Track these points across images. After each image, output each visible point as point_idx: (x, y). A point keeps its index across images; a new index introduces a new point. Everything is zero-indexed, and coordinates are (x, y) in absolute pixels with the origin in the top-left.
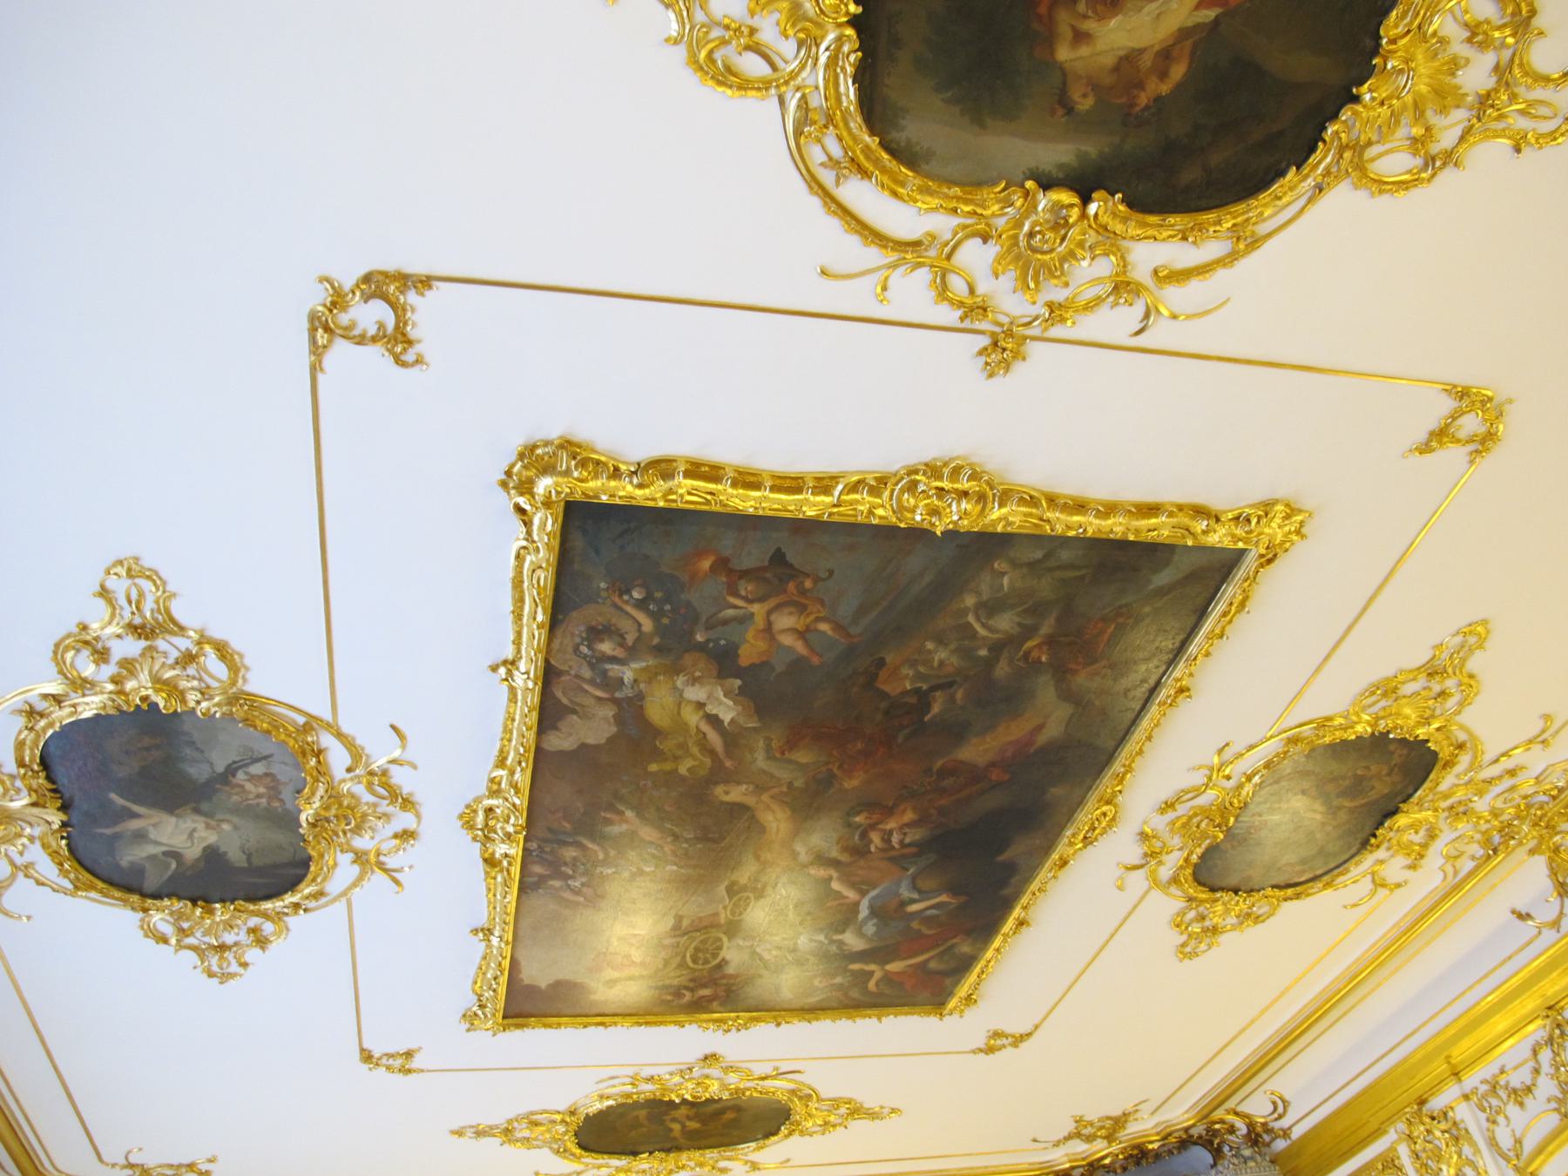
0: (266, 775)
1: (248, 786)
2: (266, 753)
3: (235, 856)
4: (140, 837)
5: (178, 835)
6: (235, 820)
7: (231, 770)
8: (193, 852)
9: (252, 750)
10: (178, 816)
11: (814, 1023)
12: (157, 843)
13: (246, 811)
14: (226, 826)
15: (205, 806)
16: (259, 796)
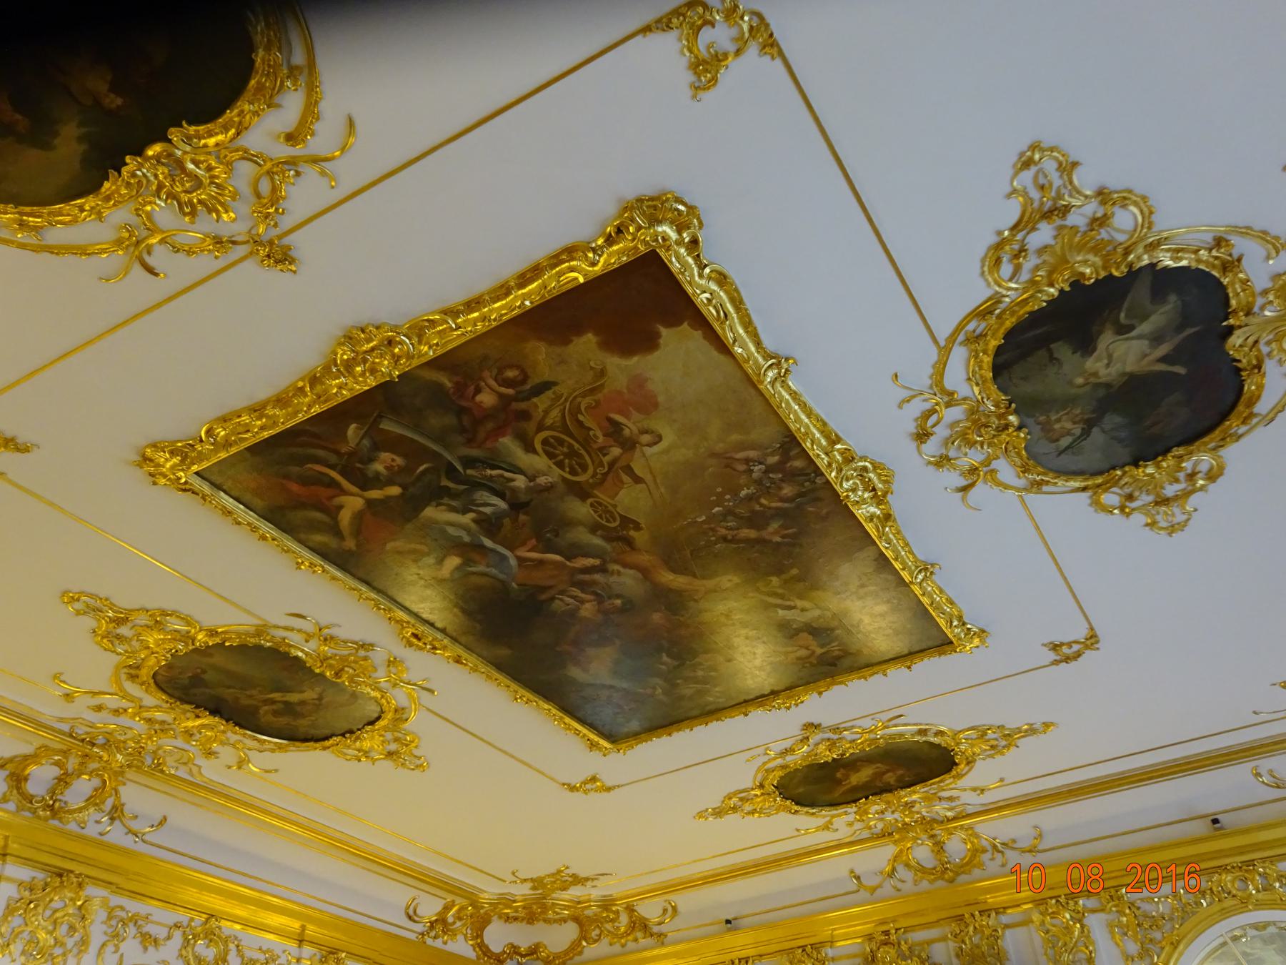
0: (1057, 440)
1: (1069, 425)
2: (1063, 456)
3: (1063, 350)
4: (1156, 339)
5: (1123, 354)
6: (1073, 391)
7: (1086, 433)
8: (1107, 340)
9: (1073, 453)
10: (1124, 374)
11: (675, 735)
12: (1139, 337)
13: (1066, 402)
14: (1080, 381)
15: (1101, 393)
16: (1059, 420)
